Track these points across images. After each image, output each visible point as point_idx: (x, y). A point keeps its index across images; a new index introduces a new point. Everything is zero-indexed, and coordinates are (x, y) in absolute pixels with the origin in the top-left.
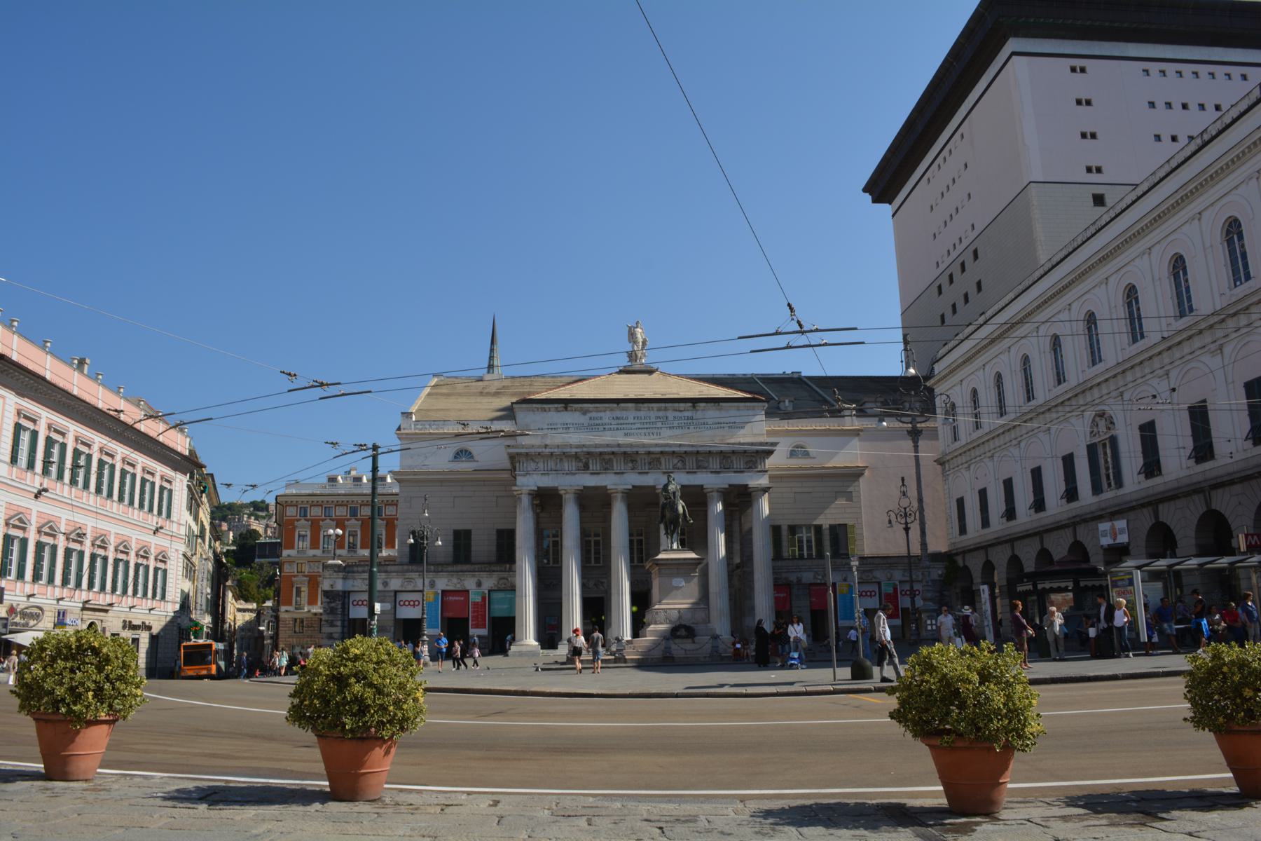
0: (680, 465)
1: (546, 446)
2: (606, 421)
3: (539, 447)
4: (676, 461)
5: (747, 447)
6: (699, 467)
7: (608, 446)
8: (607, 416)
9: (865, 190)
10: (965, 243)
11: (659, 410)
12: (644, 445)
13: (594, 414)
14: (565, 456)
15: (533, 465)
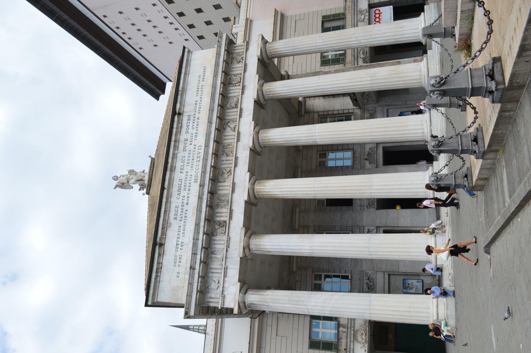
0: (232, 125)
1: (192, 268)
2: (180, 201)
3: (192, 276)
4: (228, 129)
5: (221, 60)
6: (236, 107)
7: (200, 198)
8: (175, 202)
9: (157, 98)
10: (167, 14)
11: (176, 147)
12: (205, 159)
13: (172, 215)
14: (208, 249)
15: (213, 285)
